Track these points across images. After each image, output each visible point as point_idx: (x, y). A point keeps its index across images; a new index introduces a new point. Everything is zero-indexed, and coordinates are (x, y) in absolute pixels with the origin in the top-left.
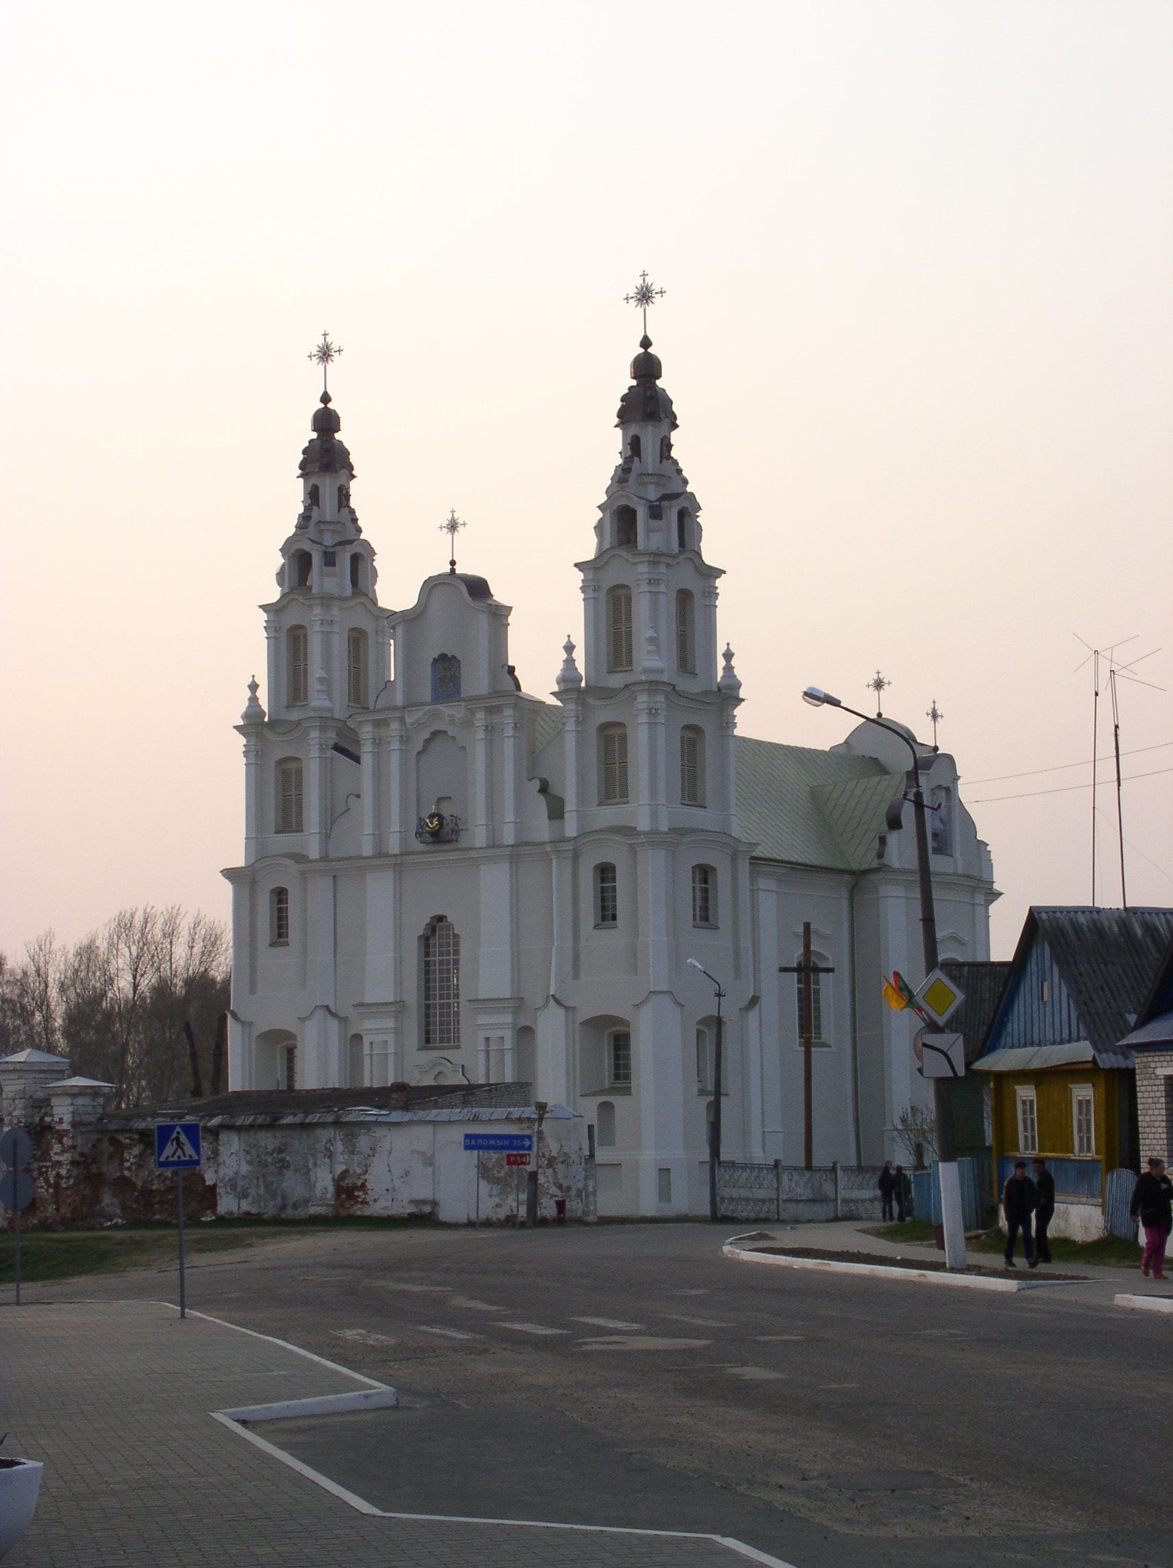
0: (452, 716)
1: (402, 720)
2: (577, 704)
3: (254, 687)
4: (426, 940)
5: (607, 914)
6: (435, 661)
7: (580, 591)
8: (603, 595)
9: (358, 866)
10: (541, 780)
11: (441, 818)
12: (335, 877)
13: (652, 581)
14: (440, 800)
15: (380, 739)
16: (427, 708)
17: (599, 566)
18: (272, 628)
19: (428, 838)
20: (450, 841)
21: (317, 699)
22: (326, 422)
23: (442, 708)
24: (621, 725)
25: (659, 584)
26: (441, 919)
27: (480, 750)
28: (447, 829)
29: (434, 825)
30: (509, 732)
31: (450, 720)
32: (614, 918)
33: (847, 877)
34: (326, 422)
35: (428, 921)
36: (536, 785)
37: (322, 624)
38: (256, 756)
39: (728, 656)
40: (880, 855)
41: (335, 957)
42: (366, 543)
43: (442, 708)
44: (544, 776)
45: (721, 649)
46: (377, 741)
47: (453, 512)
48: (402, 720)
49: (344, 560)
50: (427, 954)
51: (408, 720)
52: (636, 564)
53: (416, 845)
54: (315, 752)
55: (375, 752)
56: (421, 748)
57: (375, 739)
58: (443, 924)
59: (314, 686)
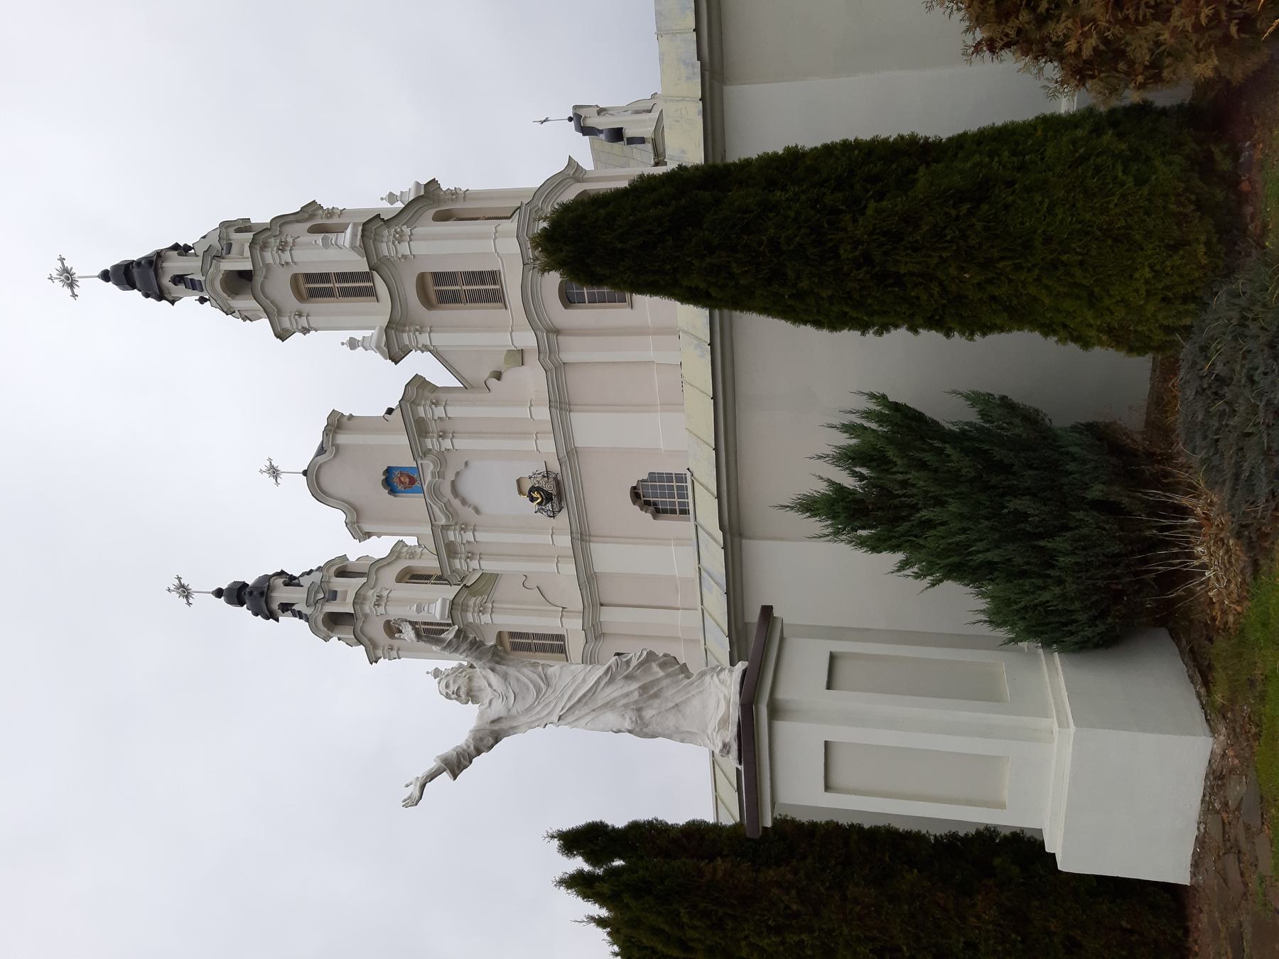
0: (433, 474)
1: (445, 528)
2: (404, 331)
4: (658, 512)
6: (393, 491)
7: (307, 335)
8: (307, 307)
9: (588, 579)
10: (490, 377)
11: (533, 489)
12: (602, 605)
13: (281, 247)
14: (521, 492)
15: (469, 553)
16: (428, 500)
17: (276, 310)
20: (555, 479)
22: (237, 594)
23: (426, 484)
24: (421, 278)
25: (286, 242)
26: (636, 495)
27: (461, 444)
29: (538, 496)
30: (439, 412)
31: (439, 478)
34: (237, 594)
35: (637, 508)
36: (493, 382)
37: (379, 605)
40: (642, 140)
41: (678, 609)
42: (330, 563)
43: (426, 484)
44: (488, 374)
45: (386, 205)
46: (470, 555)
47: (261, 471)
48: (445, 528)
49: (339, 584)
50: (673, 512)
51: (443, 521)
52: (268, 267)
54: (486, 618)
55: (480, 558)
56: (471, 510)
57: (468, 557)
58: (640, 491)
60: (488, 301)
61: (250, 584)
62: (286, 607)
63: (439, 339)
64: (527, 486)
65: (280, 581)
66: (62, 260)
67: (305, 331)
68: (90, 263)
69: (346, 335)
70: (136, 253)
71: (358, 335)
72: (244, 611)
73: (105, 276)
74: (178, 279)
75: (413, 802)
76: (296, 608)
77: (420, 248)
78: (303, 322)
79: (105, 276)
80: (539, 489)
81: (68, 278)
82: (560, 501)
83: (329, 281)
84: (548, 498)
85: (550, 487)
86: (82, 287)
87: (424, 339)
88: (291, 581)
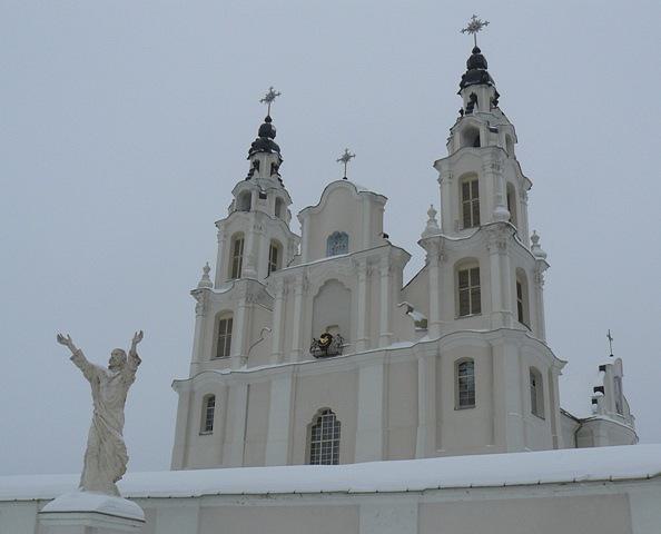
3: (207, 269)
4: (314, 429)
5: (466, 397)
6: (331, 237)
11: (330, 337)
18: (222, 236)
19: (321, 353)
20: (337, 354)
21: (247, 270)
22: (267, 131)
27: (362, 286)
28: (334, 344)
30: (385, 271)
32: (472, 402)
33: (575, 423)
34: (267, 131)
35: (315, 412)
38: (203, 309)
39: (535, 239)
49: (270, 202)
50: (313, 439)
53: (310, 359)
59: (246, 261)
60: (462, 306)
61: (274, 140)
62: (256, 165)
63: (434, 273)
64: (331, 333)
65: (276, 161)
66: (486, 24)
67: (440, 181)
68: (485, 41)
69: (438, 208)
70: (492, 70)
71: (438, 217)
72: (255, 136)
73: (476, 50)
74: (474, 98)
75: (60, 339)
76: (256, 171)
77: (495, 259)
78: (446, 180)
79: (476, 50)
80: (330, 342)
81: (475, 27)
82: (322, 356)
83: (474, 197)
84: (324, 348)
85: (332, 349)
86: (469, 37)
87: (434, 261)
88: (275, 168)
